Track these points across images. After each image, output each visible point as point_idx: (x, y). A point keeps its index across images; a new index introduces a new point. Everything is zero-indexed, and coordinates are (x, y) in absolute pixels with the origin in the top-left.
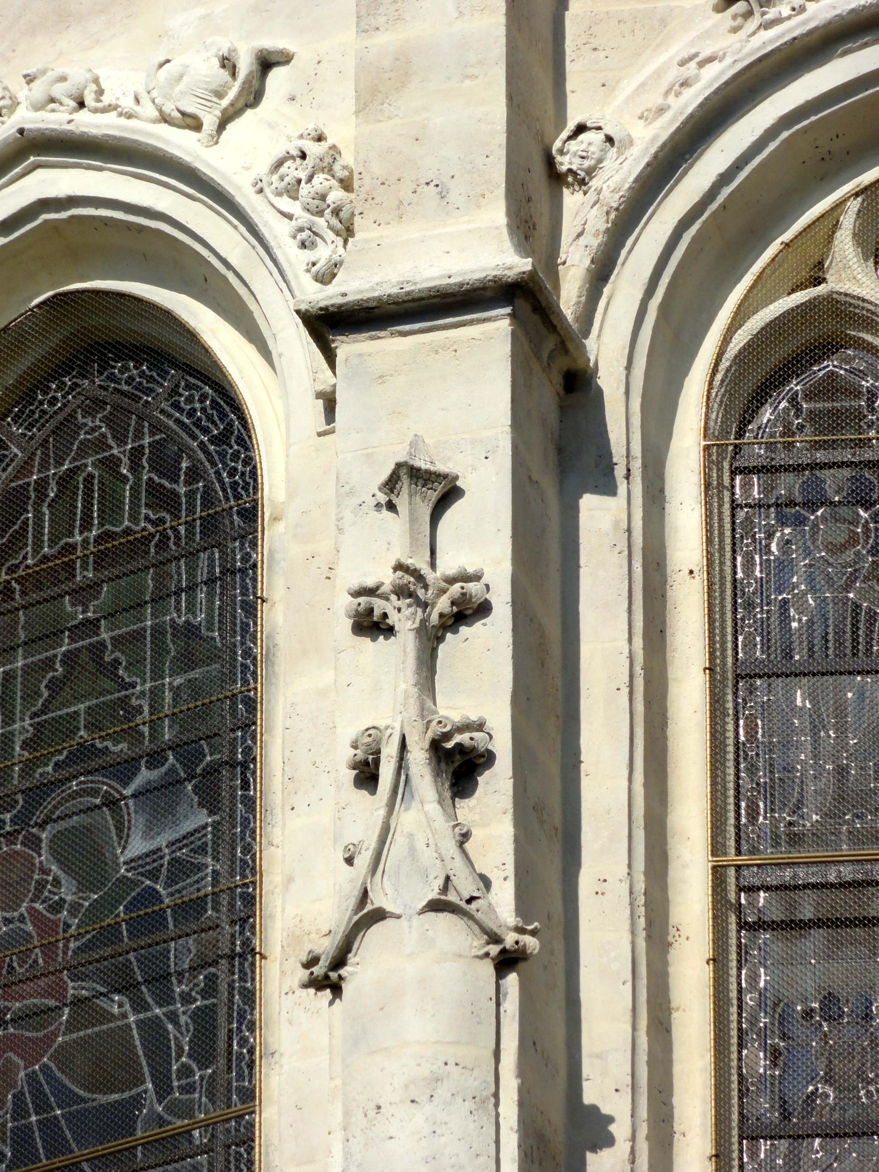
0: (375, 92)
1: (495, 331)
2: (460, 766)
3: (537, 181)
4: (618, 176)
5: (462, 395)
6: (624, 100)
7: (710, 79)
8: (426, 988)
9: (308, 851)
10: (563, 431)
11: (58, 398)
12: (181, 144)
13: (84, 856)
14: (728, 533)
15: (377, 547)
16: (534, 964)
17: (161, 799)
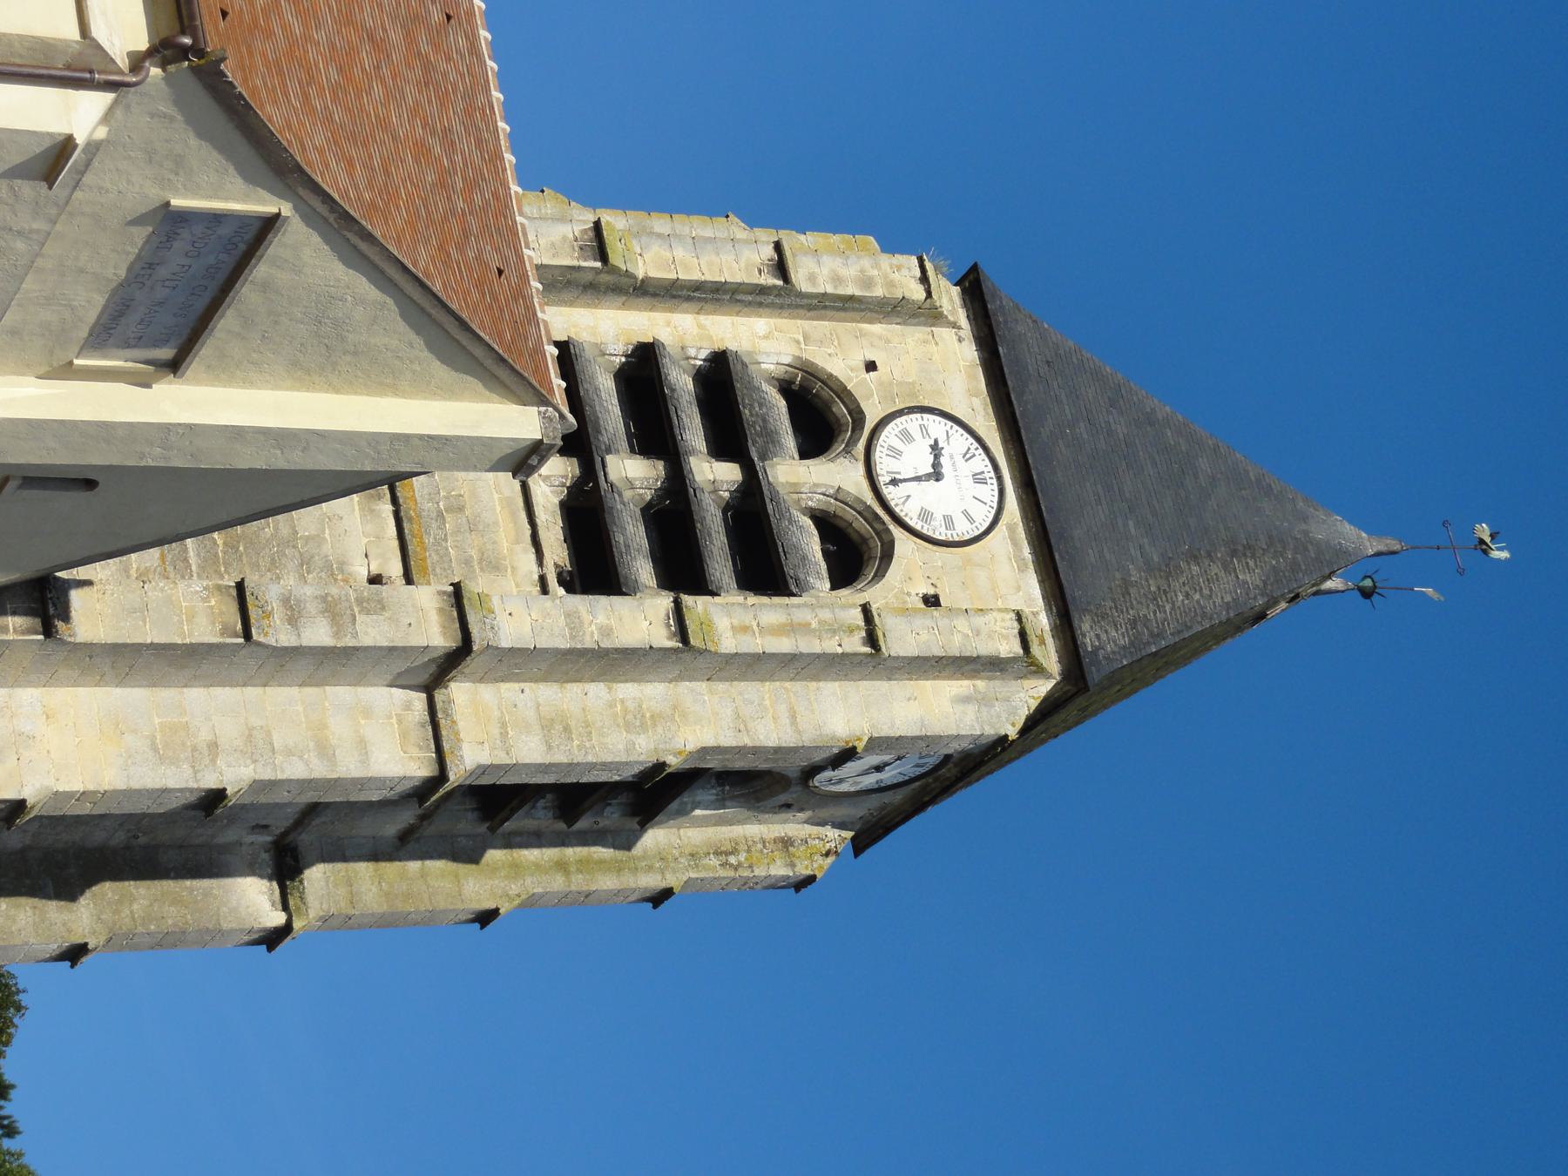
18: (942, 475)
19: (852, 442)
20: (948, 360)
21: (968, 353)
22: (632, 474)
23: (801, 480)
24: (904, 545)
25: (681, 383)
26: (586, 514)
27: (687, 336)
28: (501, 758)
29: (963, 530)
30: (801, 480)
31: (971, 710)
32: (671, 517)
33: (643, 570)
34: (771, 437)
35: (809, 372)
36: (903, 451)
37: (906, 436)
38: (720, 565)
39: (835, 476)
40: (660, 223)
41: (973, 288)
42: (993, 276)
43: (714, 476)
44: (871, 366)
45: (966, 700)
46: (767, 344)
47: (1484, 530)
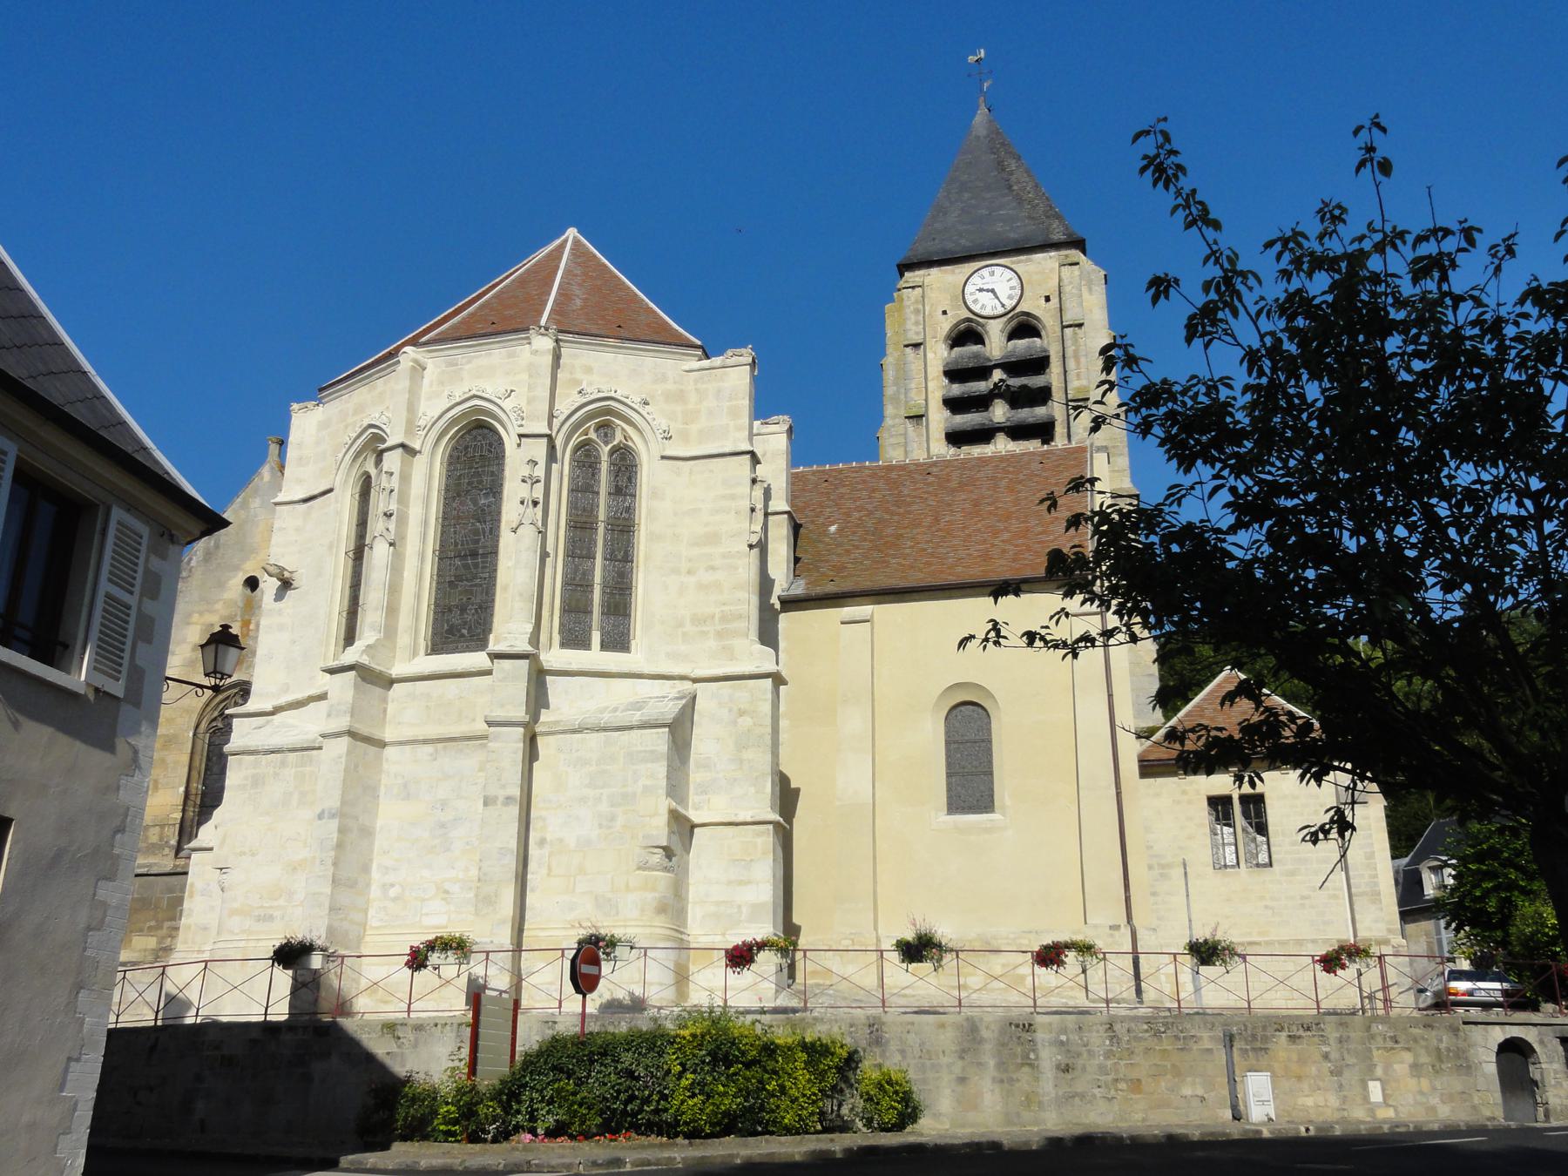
0: (529, 402)
1: (545, 440)
2: (535, 503)
3: (551, 416)
4: (562, 418)
5: (539, 449)
6: (564, 407)
8: (528, 534)
9: (510, 511)
10: (552, 456)
13: (475, 502)
14: (572, 470)
15: (526, 471)
16: (543, 533)
17: (486, 495)
18: (992, 289)
19: (978, 323)
20: (938, 280)
21: (934, 271)
22: (1000, 412)
23: (996, 345)
25: (957, 389)
26: (1018, 432)
27: (939, 387)
28: (1128, 473)
29: (1015, 282)
30: (996, 345)
31: (1095, 288)
32: (1018, 399)
34: (976, 356)
35: (948, 337)
36: (985, 305)
37: (975, 301)
38: (1035, 381)
40: (889, 391)
41: (904, 268)
42: (900, 258)
45: (1090, 290)
46: (939, 355)
47: (972, 59)
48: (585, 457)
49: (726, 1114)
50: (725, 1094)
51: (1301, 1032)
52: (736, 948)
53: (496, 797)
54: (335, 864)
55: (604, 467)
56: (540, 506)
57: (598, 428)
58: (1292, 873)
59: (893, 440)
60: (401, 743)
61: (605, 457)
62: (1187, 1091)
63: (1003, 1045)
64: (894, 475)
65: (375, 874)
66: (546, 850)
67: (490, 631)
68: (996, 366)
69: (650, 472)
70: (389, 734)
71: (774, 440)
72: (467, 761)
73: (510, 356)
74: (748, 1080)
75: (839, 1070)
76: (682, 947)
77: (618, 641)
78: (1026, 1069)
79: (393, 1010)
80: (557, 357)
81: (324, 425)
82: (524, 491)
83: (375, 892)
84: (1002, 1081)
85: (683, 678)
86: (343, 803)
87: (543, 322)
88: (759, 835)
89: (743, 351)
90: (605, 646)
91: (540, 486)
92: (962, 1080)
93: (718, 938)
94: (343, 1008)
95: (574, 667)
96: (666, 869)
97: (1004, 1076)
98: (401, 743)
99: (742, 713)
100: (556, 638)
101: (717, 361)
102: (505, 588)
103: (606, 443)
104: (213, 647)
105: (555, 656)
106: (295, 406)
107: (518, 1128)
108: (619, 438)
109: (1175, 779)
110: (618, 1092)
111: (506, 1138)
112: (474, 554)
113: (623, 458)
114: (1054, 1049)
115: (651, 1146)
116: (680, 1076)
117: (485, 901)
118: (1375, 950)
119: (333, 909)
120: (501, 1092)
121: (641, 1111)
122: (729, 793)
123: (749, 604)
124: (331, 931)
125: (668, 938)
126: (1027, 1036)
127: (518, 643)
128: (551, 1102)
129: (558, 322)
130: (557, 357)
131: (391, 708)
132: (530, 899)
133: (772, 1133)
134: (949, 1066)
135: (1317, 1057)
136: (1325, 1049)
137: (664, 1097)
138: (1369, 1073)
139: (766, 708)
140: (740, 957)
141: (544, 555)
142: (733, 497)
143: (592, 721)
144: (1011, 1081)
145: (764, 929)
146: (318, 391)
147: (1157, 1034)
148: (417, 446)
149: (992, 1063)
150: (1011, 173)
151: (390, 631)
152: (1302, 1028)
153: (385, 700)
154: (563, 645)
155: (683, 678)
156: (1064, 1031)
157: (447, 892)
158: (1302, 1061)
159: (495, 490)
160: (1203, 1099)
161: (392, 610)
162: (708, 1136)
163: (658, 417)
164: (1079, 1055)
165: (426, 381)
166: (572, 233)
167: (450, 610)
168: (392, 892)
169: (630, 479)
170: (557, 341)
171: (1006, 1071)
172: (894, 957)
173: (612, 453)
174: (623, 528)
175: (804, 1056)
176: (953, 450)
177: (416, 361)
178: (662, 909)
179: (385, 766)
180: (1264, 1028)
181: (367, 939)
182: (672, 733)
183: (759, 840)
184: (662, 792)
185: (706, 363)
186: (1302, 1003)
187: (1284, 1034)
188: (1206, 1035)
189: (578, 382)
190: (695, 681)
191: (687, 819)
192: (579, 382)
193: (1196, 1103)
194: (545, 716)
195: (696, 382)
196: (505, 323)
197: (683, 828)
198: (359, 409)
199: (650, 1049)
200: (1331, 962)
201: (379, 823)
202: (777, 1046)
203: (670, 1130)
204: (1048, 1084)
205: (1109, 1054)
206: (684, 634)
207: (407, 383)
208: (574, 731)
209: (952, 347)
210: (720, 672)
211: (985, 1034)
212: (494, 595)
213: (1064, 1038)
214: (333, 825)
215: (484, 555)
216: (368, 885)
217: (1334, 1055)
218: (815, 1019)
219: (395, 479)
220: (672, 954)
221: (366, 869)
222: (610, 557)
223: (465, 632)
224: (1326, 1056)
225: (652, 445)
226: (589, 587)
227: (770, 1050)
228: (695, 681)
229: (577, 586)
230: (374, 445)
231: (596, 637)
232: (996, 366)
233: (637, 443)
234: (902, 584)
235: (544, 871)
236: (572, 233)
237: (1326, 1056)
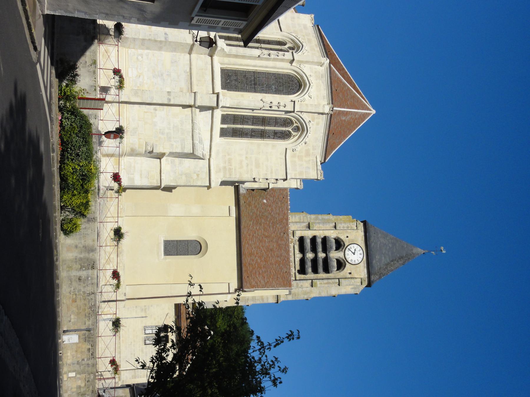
0: (307, 105)
1: (293, 110)
2: (271, 107)
5: (290, 108)
6: (305, 116)
7: (305, 120)
10: (287, 112)
11: (298, 84)
12: (308, 93)
13: (273, 84)
14: (284, 118)
15: (282, 104)
18: (355, 255)
19: (343, 249)
20: (359, 235)
22: (310, 255)
23: (334, 255)
24: (347, 264)
25: (319, 241)
26: (303, 262)
27: (320, 234)
28: (286, 299)
29: (357, 262)
30: (334, 255)
32: (315, 261)
33: (310, 270)
34: (331, 248)
35: (339, 238)
39: (339, 255)
40: (320, 217)
41: (365, 223)
42: (369, 221)
43: (321, 255)
44: (347, 237)
45: (352, 288)
46: (332, 234)
47: (442, 248)
48: (287, 122)
49: (67, 179)
50: (73, 178)
51: (91, 352)
52: (119, 176)
53: (170, 96)
54: (149, 40)
55: (284, 129)
56: (270, 109)
57: (298, 127)
58: (142, 351)
59: (302, 217)
60: (190, 60)
61: (287, 129)
62: (72, 317)
63: (87, 260)
64: (284, 221)
65: (146, 51)
66: (152, 111)
67: (228, 90)
68: (327, 255)
69: (281, 144)
70: (193, 55)
71: (294, 184)
72: (184, 84)
73: (324, 97)
74: (77, 185)
75: (80, 212)
76: (120, 156)
77: (224, 133)
78: (80, 267)
79: (101, 61)
80: (322, 114)
81: (305, 27)
82: (275, 103)
83: (140, 51)
84: (76, 259)
85: (210, 155)
86: (170, 42)
87: (335, 109)
88: (157, 181)
89: (322, 176)
90: (222, 129)
91: (277, 109)
92: (76, 247)
93: (123, 167)
94: (101, 42)
95: (215, 119)
96: (146, 151)
97: (77, 260)
98: (190, 60)
99: (198, 175)
100: (225, 113)
101: (320, 167)
102: (242, 96)
103: (292, 129)
104: (208, 40)
105: (218, 114)
106: (313, 16)
107: (63, 114)
108: (294, 133)
109: (174, 315)
110: (74, 146)
111: (60, 111)
112: (255, 84)
113: (287, 135)
114: (86, 275)
115: (57, 157)
116: (79, 165)
117: (136, 93)
118: (117, 376)
119: (134, 39)
120: (74, 109)
121: (68, 153)
122: (171, 171)
123: (235, 178)
124: (127, 38)
125: (123, 152)
126: (90, 267)
127: (222, 102)
128: (71, 125)
129: (335, 114)
130: (322, 114)
131: (203, 56)
132: (136, 106)
133: (61, 192)
134: (81, 243)
135: (83, 357)
136: (86, 360)
137: (72, 160)
138: (78, 373)
139: (199, 184)
140: (116, 177)
141: (253, 110)
142: (272, 173)
143: (196, 127)
144: (76, 262)
145: (125, 182)
146: (317, 25)
147: (91, 308)
148: (294, 64)
149: (82, 256)
150: (398, 261)
151: (229, 56)
152: (92, 353)
153: (205, 54)
154: (223, 115)
155: (210, 155)
156: (92, 279)
157: (139, 77)
158: (82, 352)
159: (277, 92)
160: (70, 321)
161: (236, 56)
162: (60, 173)
163: (300, 147)
164: (84, 283)
165: (317, 67)
166: (374, 112)
167: (236, 76)
168: (140, 57)
169: (280, 137)
170: (328, 114)
171: (79, 260)
172: (116, 226)
173: (289, 131)
174: (262, 135)
175: (84, 202)
176: (297, 239)
177: (324, 64)
178: (133, 150)
179: (183, 54)
180: (92, 341)
181: (124, 49)
182: (191, 153)
183: (155, 181)
184: (171, 151)
185: (319, 163)
186: (100, 353)
187: (90, 347)
188: (90, 323)
189: (313, 120)
190: (209, 160)
191: (163, 157)
192: (313, 121)
193: (69, 319)
194: (198, 110)
195: (313, 160)
196: (336, 93)
197: (160, 157)
198: (309, 41)
199: (87, 156)
200: (113, 362)
201: (163, 52)
202: (88, 194)
203: (62, 162)
204: (75, 273)
205: (84, 293)
206: (225, 156)
207: (316, 61)
208: (192, 120)
209: (335, 239)
210: (212, 168)
211: (91, 254)
212: (241, 91)
213: (90, 279)
214: (163, 39)
215: (255, 88)
216: (143, 49)
217: (83, 362)
218: (96, 201)
219: (282, 57)
220: (118, 153)
221: (148, 48)
222: (253, 130)
223: (228, 81)
224: (83, 360)
225: (291, 145)
226: (243, 124)
227: (87, 192)
228: (209, 160)
229: (243, 119)
230: (296, 47)
231: (225, 126)
232: (327, 255)
233: (292, 140)
234: (242, 227)
235: (146, 110)
236: (374, 112)
237: (83, 360)
